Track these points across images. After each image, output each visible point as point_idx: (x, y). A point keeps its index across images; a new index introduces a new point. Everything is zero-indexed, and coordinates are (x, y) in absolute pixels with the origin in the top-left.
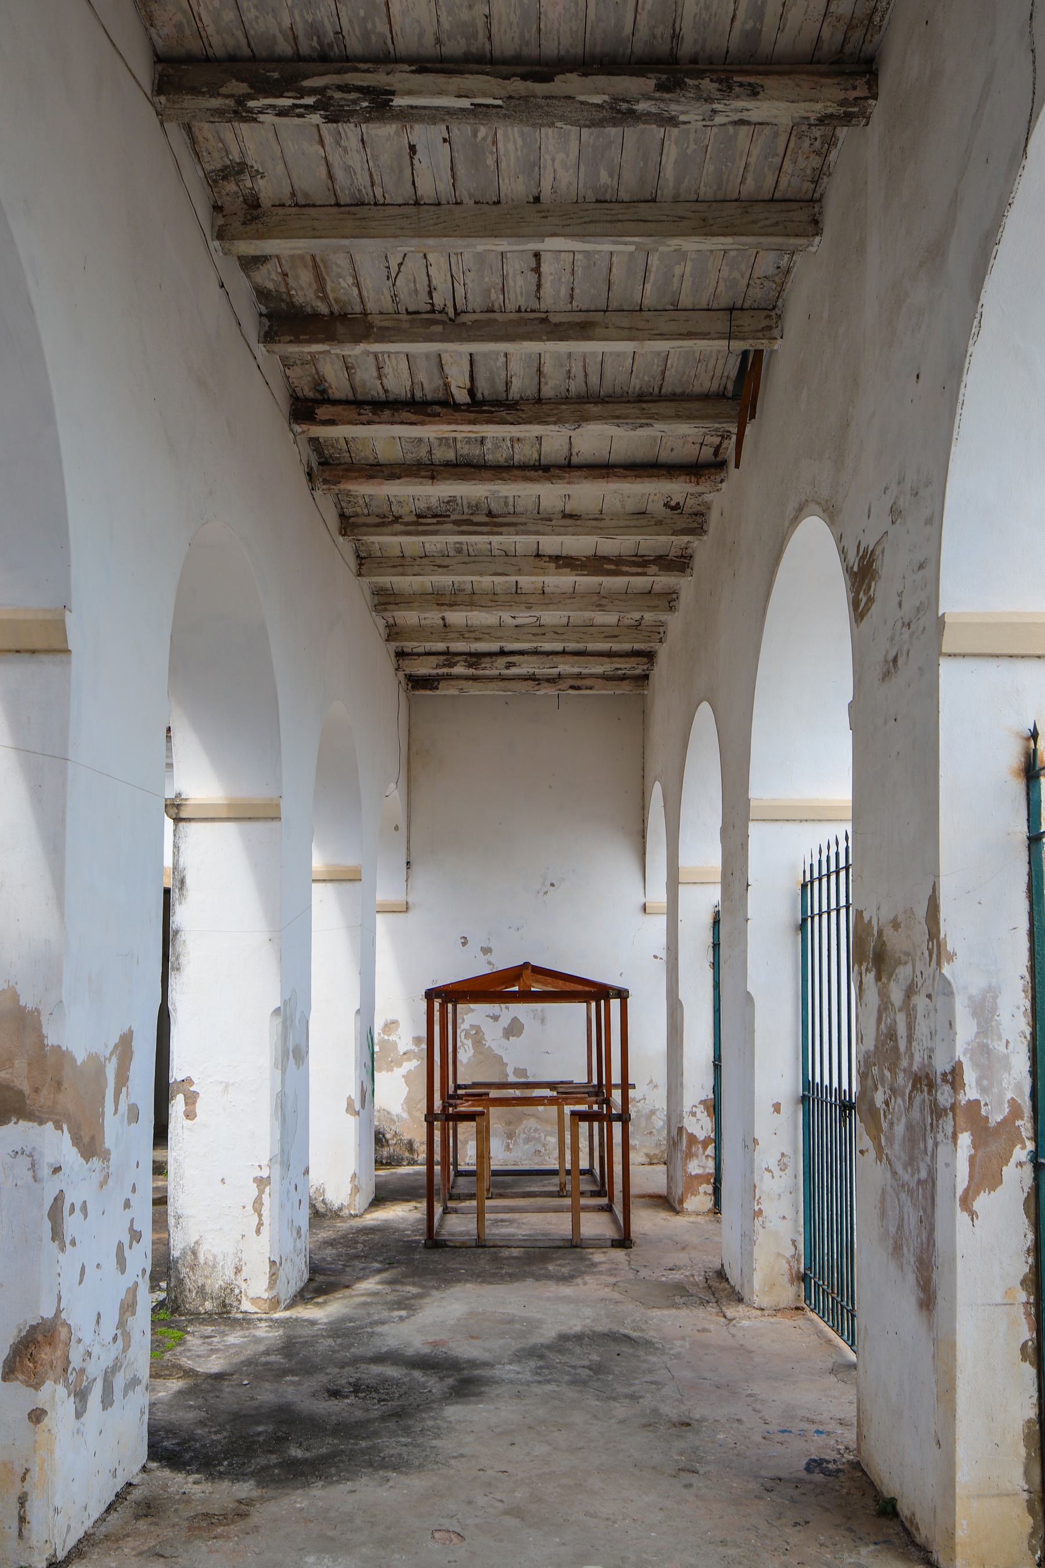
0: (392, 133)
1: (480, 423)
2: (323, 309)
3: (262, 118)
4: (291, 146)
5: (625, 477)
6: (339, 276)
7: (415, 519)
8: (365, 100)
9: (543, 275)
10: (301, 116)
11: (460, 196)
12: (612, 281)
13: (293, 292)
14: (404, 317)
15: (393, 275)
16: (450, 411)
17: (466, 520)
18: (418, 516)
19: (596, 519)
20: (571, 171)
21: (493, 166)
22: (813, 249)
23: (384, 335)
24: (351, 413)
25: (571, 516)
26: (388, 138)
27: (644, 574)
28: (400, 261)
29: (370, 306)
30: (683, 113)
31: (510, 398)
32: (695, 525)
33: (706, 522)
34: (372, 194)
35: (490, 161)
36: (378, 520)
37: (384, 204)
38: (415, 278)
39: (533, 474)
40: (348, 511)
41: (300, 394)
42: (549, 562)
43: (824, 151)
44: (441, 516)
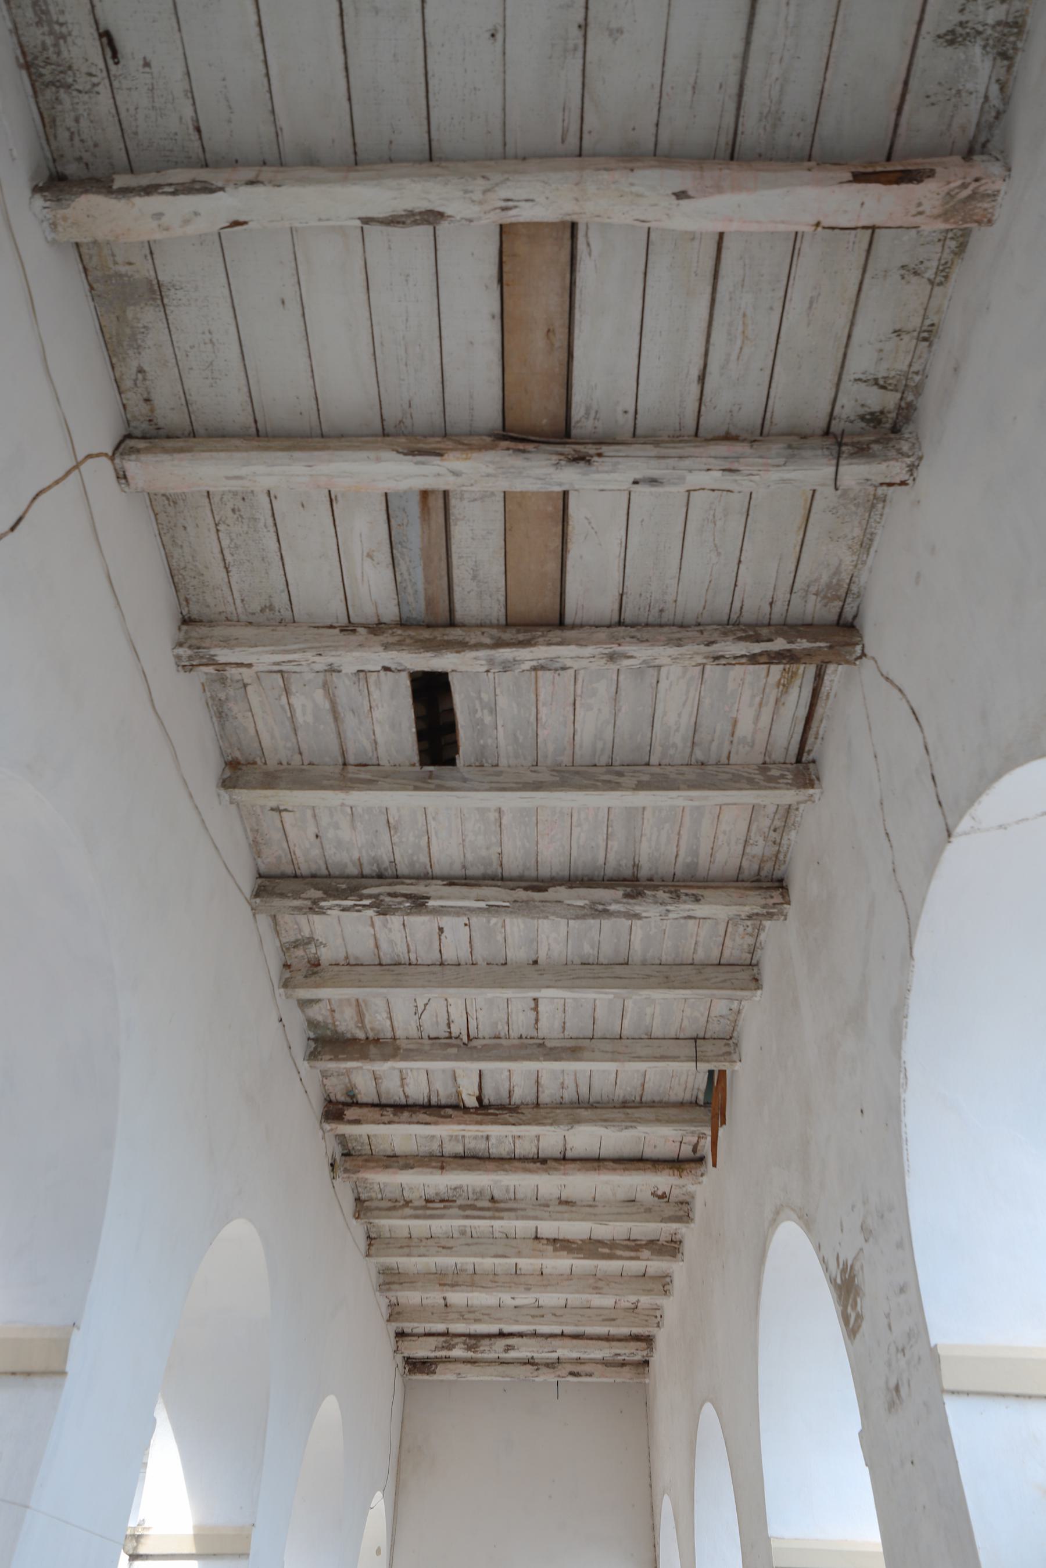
1: (486, 1123)
2: (361, 1035)
3: (329, 912)
5: (614, 1170)
7: (424, 1203)
8: (407, 902)
10: (359, 911)
13: (337, 1023)
14: (426, 1041)
15: (420, 1012)
16: (460, 1113)
17: (471, 1205)
18: (427, 1201)
19: (590, 1206)
21: (502, 940)
22: (757, 999)
23: (409, 1055)
24: (375, 1113)
25: (567, 1203)
27: (637, 1258)
28: (426, 1002)
29: (399, 1033)
30: (645, 911)
31: (512, 1103)
32: (681, 1213)
33: (691, 1210)
35: (500, 938)
36: (390, 1204)
37: (416, 965)
39: (531, 1165)
40: (363, 1197)
41: (333, 1098)
42: (547, 1244)
43: (756, 934)
44: (448, 1201)
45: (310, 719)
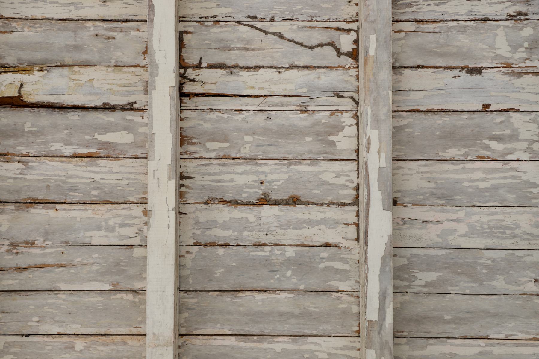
0: (498, 52)
9: (256, 209)
11: (400, 116)
12: (240, 295)
20: (440, 240)
26: (492, 47)
34: (403, 17)
35: (452, 152)
38: (253, 50)
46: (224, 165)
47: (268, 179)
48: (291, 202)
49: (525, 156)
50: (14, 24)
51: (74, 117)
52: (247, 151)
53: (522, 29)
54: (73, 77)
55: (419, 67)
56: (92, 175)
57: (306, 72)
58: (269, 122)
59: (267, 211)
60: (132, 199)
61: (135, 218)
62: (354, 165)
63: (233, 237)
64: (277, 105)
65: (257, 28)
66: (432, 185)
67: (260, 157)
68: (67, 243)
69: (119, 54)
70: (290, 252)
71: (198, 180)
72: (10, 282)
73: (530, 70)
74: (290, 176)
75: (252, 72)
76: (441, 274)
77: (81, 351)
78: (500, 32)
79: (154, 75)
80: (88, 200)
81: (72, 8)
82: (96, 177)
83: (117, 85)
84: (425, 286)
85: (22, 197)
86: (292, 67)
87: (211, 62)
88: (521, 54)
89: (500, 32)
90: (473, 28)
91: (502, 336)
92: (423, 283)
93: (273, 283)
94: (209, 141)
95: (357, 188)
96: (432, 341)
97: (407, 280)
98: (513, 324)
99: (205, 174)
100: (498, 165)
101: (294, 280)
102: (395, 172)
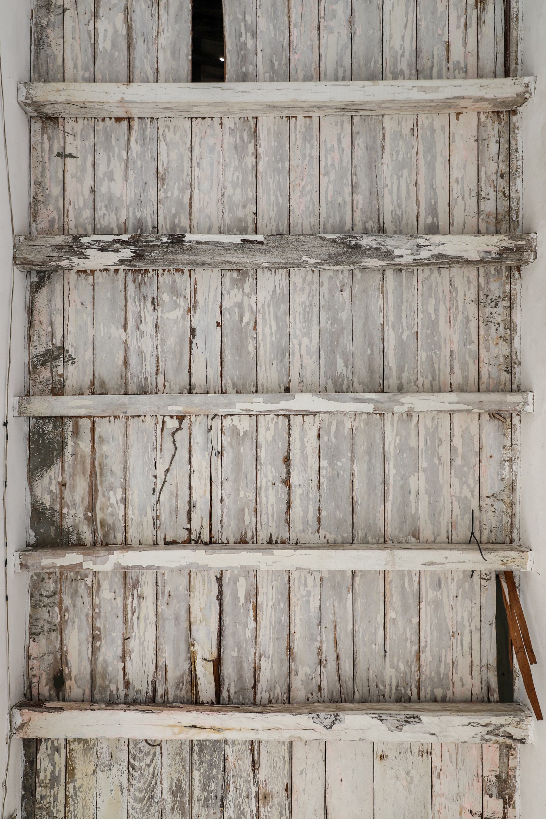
0: (179, 317)
4: (102, 329)
6: (111, 488)
9: (293, 488)
11: (225, 385)
12: (355, 499)
13: (65, 511)
20: (314, 357)
26: (176, 321)
34: (154, 383)
35: (251, 348)
38: (177, 491)
45: (108, 45)
46: (261, 511)
47: (271, 480)
48: (288, 463)
49: (254, 298)
50: (160, 664)
51: (227, 621)
52: (251, 495)
53: (164, 301)
54: (198, 622)
55: (190, 372)
56: (269, 608)
57: (193, 452)
58: (230, 479)
59: (294, 480)
60: (287, 578)
61: (300, 576)
62: (261, 418)
63: (314, 505)
64: (218, 473)
65: (162, 488)
66: (274, 362)
67: (255, 486)
68: (319, 624)
69: (181, 588)
70: (324, 463)
71: (273, 530)
72: (347, 665)
73: (193, 295)
74: (269, 464)
75: (194, 492)
76: (338, 356)
77: (396, 613)
78: (165, 316)
79: (197, 566)
80: (287, 609)
81: (148, 622)
82: (270, 604)
83: (204, 589)
84: (347, 367)
85: (286, 658)
86: (190, 463)
87: (187, 521)
88: (181, 301)
89: (165, 316)
90: (162, 335)
91: (381, 314)
92: (345, 368)
93: (347, 476)
94: (244, 522)
95: (278, 415)
96: (386, 363)
97: (343, 380)
98: (373, 307)
99: (268, 525)
100: (260, 316)
101: (344, 460)
102: (265, 390)
